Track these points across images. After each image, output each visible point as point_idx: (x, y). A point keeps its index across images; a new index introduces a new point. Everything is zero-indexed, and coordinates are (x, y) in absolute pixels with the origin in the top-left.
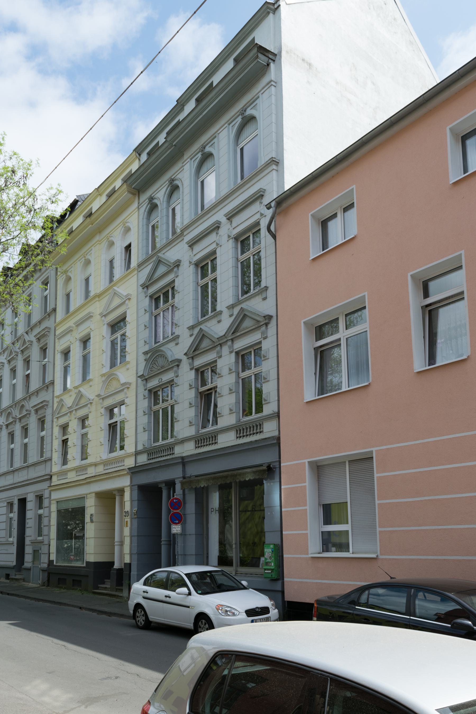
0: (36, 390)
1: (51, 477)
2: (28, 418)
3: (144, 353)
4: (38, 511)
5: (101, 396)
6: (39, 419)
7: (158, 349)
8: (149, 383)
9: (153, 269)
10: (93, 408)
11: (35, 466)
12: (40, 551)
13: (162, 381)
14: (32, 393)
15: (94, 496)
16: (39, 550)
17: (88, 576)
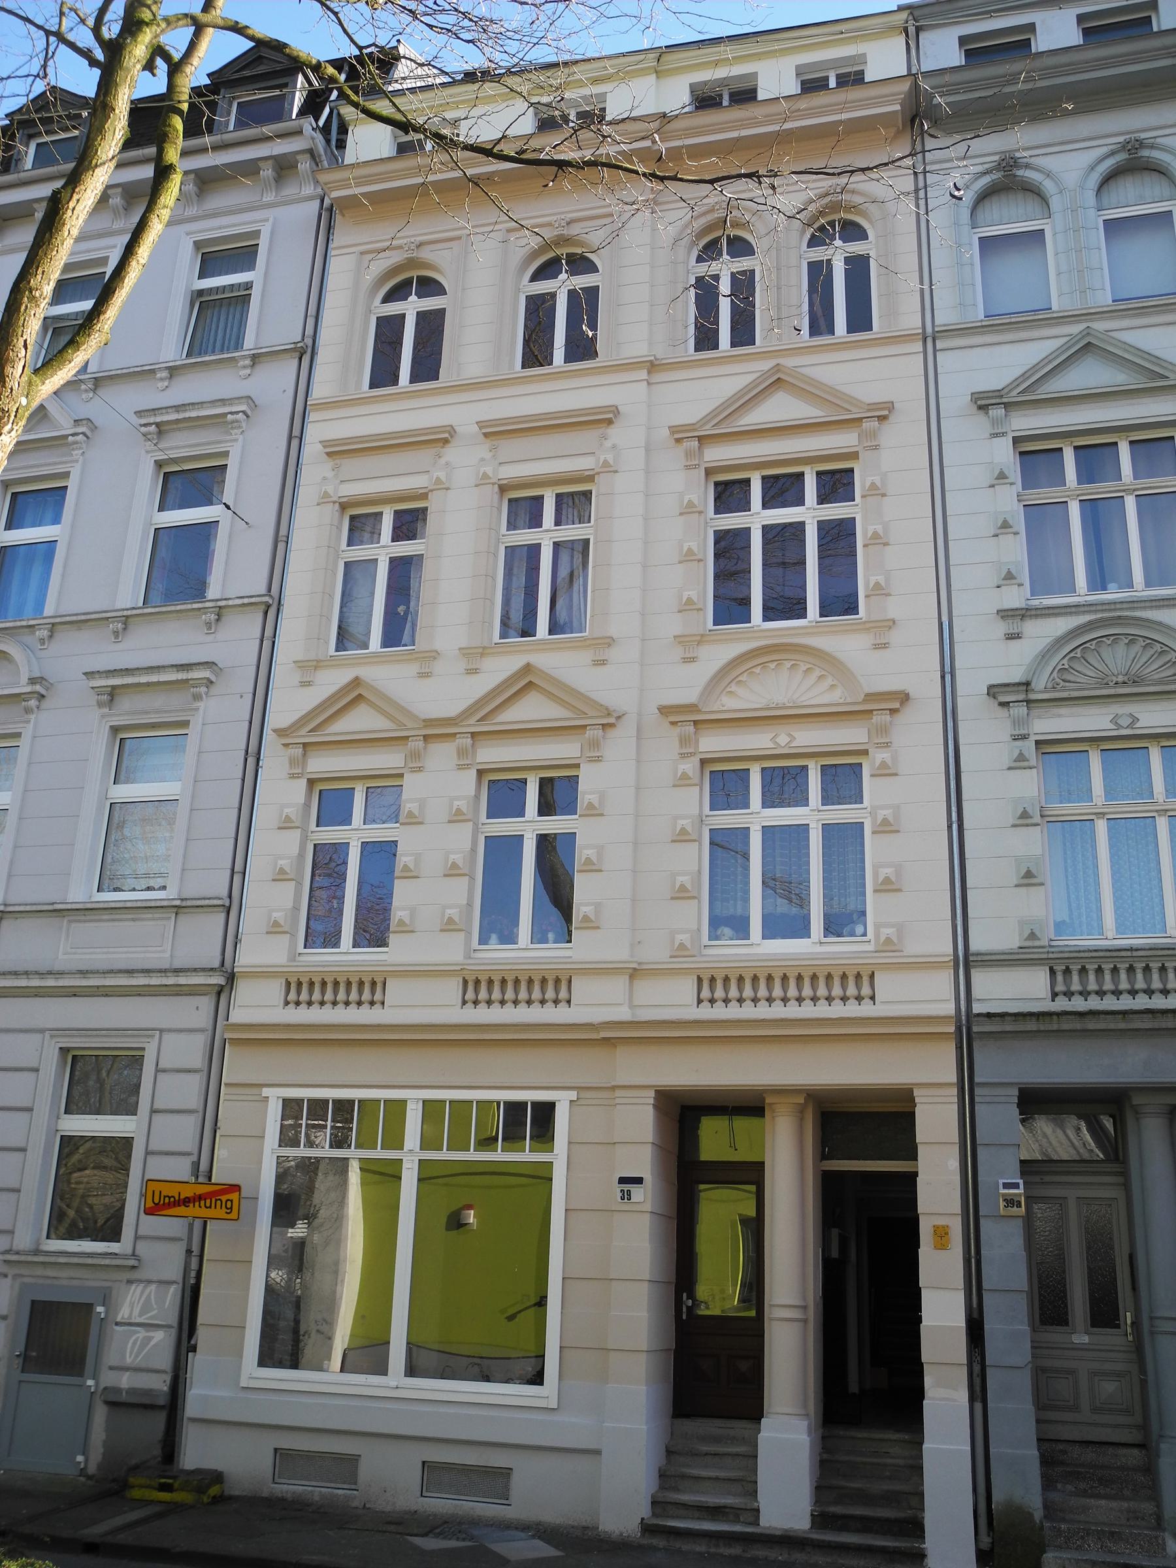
0: (125, 613)
1: (231, 978)
2: (28, 711)
3: (1003, 614)
4: (58, 1118)
5: (699, 711)
6: (115, 730)
7: (1138, 614)
8: (1039, 717)
9: (1050, 362)
10: (619, 745)
11: (70, 922)
12: (100, 1309)
13: (1137, 725)
14: (83, 617)
15: (652, 1101)
16: (89, 1307)
17: (597, 1452)
